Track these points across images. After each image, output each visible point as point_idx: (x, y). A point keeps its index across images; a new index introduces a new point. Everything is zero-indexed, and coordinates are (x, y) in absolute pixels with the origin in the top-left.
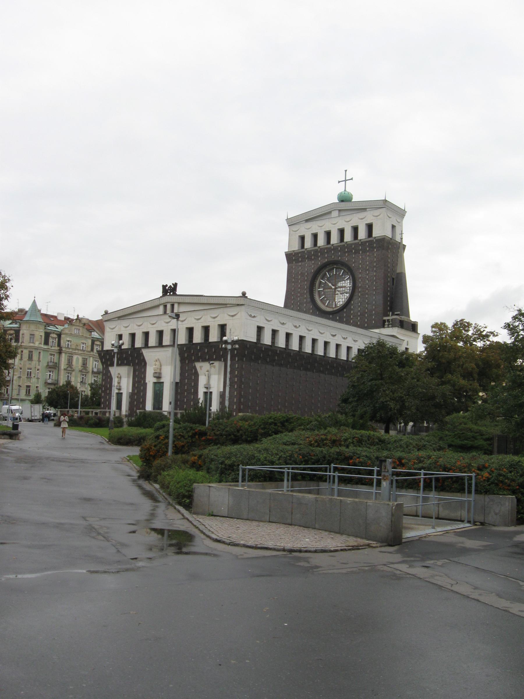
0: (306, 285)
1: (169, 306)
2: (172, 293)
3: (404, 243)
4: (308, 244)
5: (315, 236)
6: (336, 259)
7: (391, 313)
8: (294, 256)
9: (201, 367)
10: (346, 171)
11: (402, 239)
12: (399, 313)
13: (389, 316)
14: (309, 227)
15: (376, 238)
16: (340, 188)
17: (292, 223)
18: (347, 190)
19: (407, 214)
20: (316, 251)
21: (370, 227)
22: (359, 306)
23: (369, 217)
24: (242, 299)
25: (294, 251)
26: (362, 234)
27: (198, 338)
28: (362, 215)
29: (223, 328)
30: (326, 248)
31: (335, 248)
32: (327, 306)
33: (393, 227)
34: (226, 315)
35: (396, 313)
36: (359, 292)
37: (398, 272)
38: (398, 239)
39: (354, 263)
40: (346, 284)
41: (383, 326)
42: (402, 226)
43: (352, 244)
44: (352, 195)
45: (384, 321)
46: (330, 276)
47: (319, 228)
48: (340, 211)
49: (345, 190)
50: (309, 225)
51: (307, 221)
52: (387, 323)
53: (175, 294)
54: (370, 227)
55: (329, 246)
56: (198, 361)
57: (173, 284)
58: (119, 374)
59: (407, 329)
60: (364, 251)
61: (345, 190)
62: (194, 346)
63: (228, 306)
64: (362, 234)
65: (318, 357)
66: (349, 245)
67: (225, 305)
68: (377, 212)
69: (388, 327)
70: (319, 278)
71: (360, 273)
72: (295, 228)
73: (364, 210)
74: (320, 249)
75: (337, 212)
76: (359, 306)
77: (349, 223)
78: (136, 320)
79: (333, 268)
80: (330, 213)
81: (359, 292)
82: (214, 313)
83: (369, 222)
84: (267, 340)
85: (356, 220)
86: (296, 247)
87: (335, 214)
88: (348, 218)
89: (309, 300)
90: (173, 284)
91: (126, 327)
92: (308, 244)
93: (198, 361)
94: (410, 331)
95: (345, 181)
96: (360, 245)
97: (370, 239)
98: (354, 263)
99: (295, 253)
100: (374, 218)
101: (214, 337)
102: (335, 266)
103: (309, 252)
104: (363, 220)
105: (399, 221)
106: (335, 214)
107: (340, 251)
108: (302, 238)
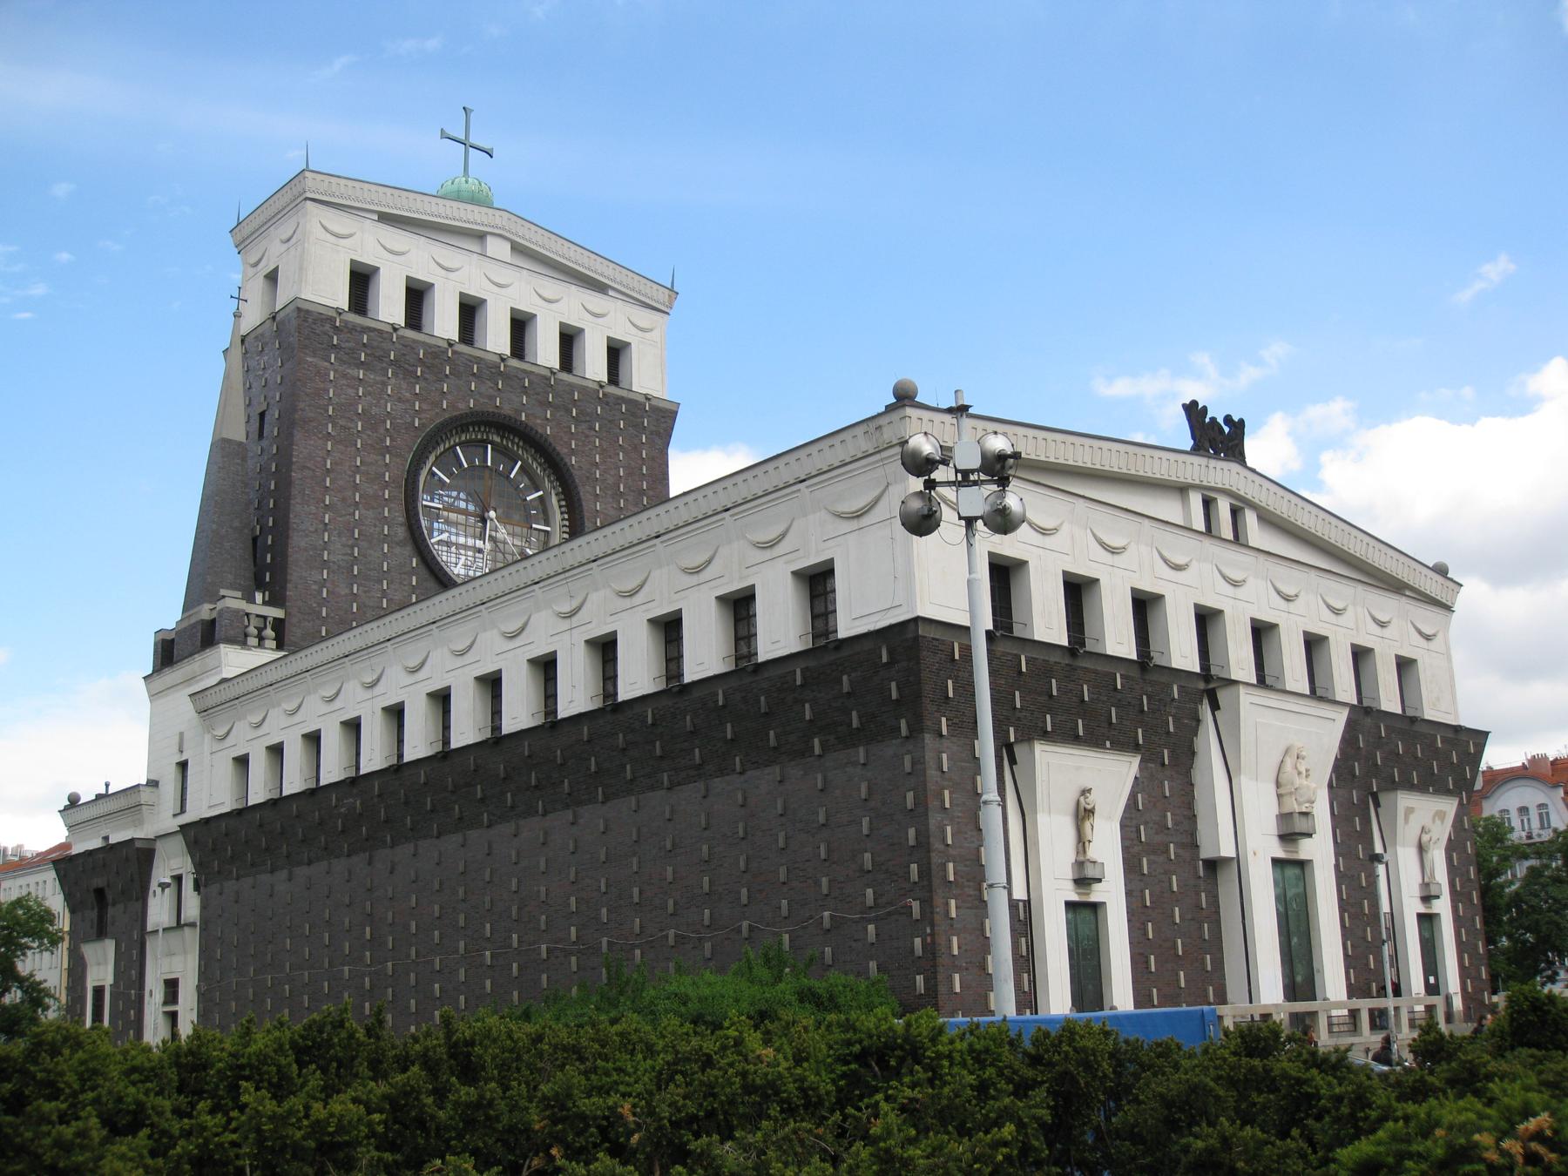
0: (393, 468)
6: (507, 410)
9: (1409, 811)
14: (397, 248)
15: (654, 402)
26: (594, 366)
31: (491, 370)
39: (573, 452)
51: (386, 218)
57: (1228, 419)
58: (1085, 792)
64: (594, 366)
68: (644, 317)
70: (432, 458)
73: (600, 287)
78: (1099, 516)
85: (571, 306)
88: (553, 287)
92: (389, 307)
100: (634, 331)
102: (497, 439)
107: (525, 390)
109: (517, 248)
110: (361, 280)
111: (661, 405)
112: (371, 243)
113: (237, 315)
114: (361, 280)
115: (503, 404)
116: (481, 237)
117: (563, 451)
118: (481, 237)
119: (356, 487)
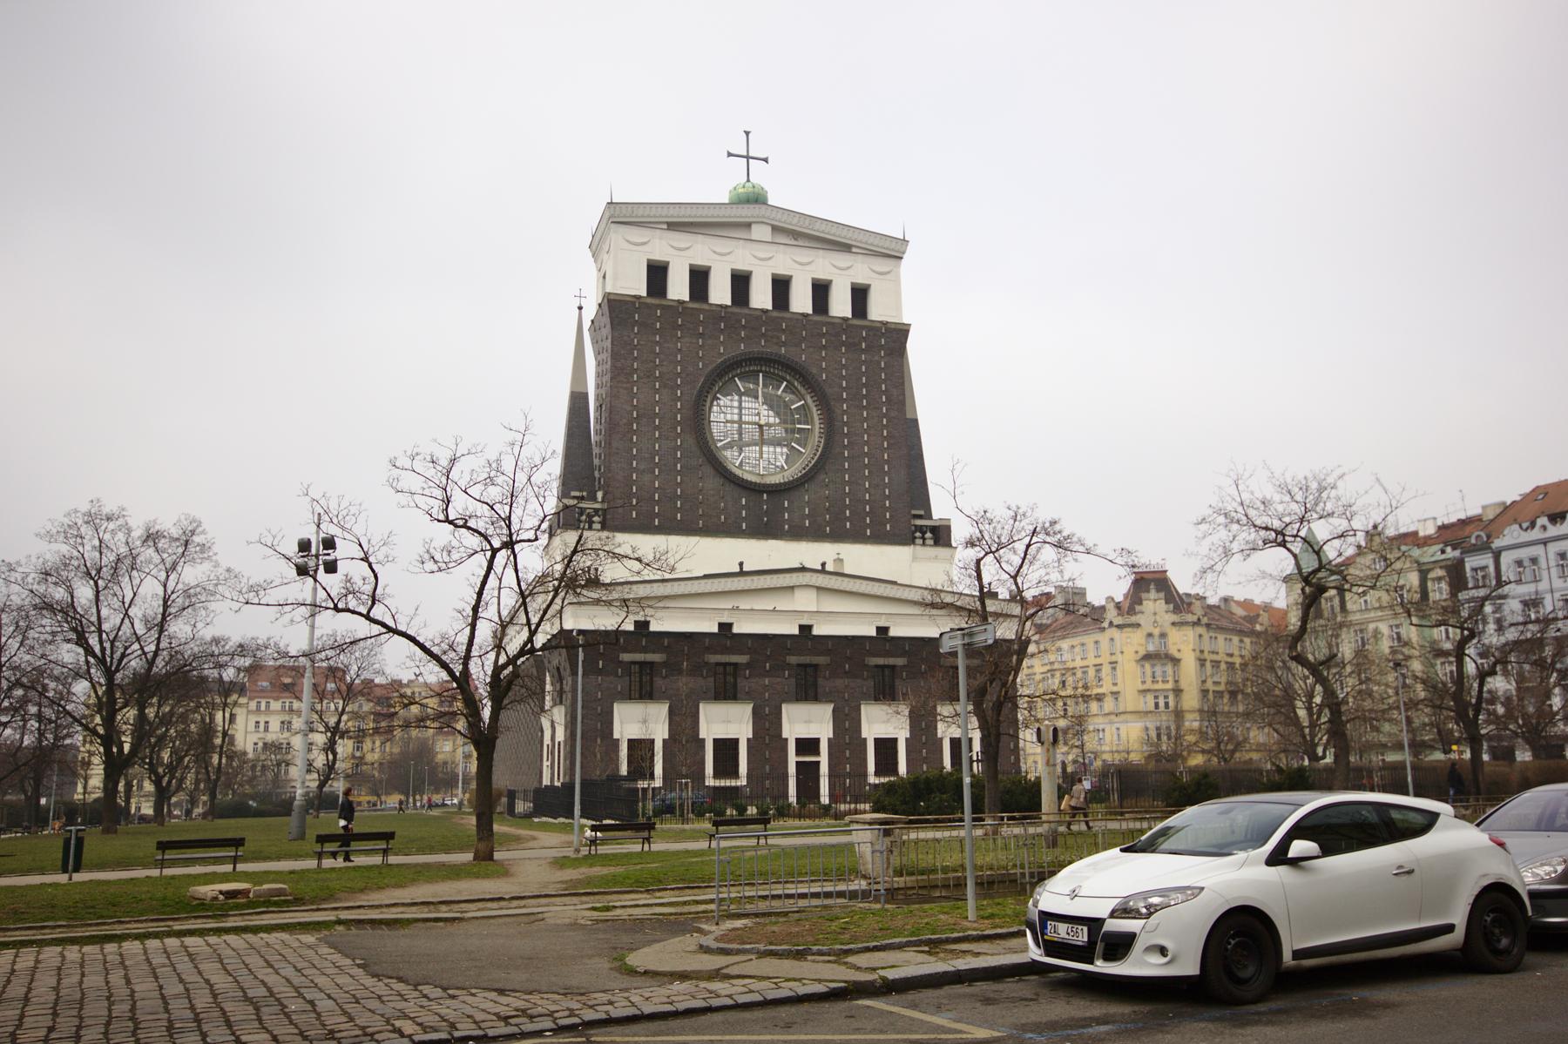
4: (678, 288)
5: (699, 278)
10: (747, 133)
14: (683, 245)
17: (621, 216)
21: (860, 295)
26: (841, 306)
28: (842, 259)
47: (721, 259)
48: (775, 229)
51: (673, 226)
54: (860, 295)
60: (853, 346)
64: (841, 306)
68: (882, 265)
73: (845, 248)
83: (861, 280)
85: (823, 265)
86: (637, 285)
87: (761, 232)
88: (804, 255)
92: (678, 288)
106: (761, 232)
109: (776, 229)
110: (657, 273)
112: (661, 247)
113: (580, 308)
114: (657, 273)
115: (762, 346)
116: (748, 225)
117: (814, 371)
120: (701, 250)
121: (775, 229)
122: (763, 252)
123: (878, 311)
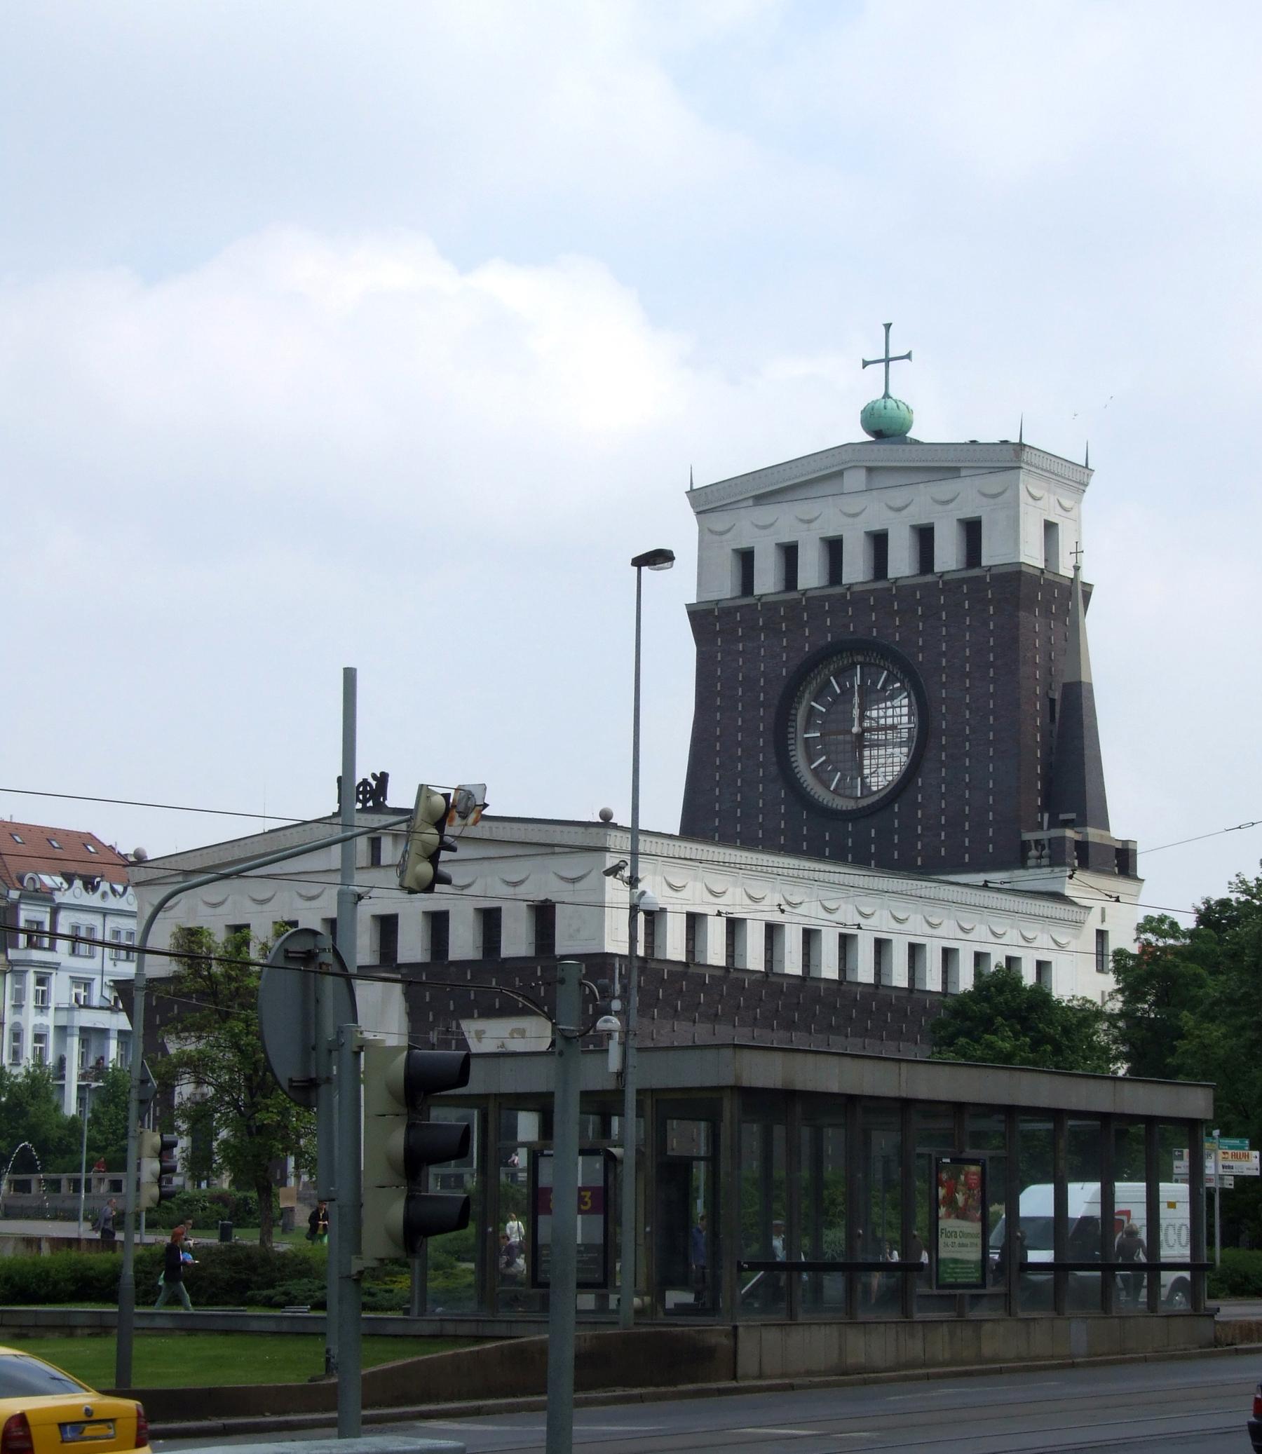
1: (362, 844)
2: (370, 804)
3: (1085, 577)
4: (767, 581)
7: (1046, 816)
8: (718, 618)
9: (480, 1035)
10: (888, 326)
11: (1077, 568)
12: (1072, 816)
13: (1040, 826)
15: (994, 571)
16: (869, 389)
18: (891, 393)
19: (1094, 481)
20: (793, 606)
22: (943, 796)
23: (968, 497)
24: (602, 831)
25: (718, 601)
26: (948, 556)
27: (464, 943)
28: (945, 488)
29: (544, 914)
30: (828, 598)
31: (858, 598)
32: (835, 792)
33: (1050, 527)
34: (552, 876)
35: (1062, 817)
36: (943, 748)
37: (1067, 679)
38: (1066, 570)
39: (922, 649)
40: (897, 713)
41: (1022, 863)
42: (1078, 521)
43: (914, 588)
44: (910, 411)
45: (1025, 846)
46: (842, 692)
48: (870, 470)
49: (887, 395)
50: (766, 513)
51: (760, 499)
52: (1033, 853)
53: (380, 808)
55: (837, 590)
56: (471, 1017)
57: (374, 776)
59: (1100, 871)
61: (887, 395)
62: (453, 969)
63: (557, 849)
64: (948, 556)
65: (822, 986)
66: (904, 591)
67: (549, 848)
68: (993, 483)
69: (1039, 866)
70: (807, 696)
71: (943, 685)
72: (719, 521)
73: (953, 472)
74: (808, 599)
75: (862, 474)
76: (943, 796)
77: (905, 512)
79: (854, 665)
80: (839, 474)
81: (943, 748)
82: (515, 870)
83: (969, 513)
84: (674, 948)
87: (855, 480)
88: (898, 497)
89: (774, 769)
90: (374, 776)
91: (215, 905)
92: (767, 581)
93: (467, 1012)
94: (1113, 874)
95: (887, 361)
96: (942, 591)
97: (975, 572)
98: (922, 649)
99: (722, 610)
101: (517, 941)
102: (860, 658)
103: (770, 607)
104: (951, 506)
105: (1066, 503)
106: (855, 480)
107: (873, 608)
108: (746, 558)
111: (1002, 570)
118: (839, 474)
119: (739, 744)
120: (786, 522)
121: (870, 470)
122: (852, 504)
123: (991, 555)
